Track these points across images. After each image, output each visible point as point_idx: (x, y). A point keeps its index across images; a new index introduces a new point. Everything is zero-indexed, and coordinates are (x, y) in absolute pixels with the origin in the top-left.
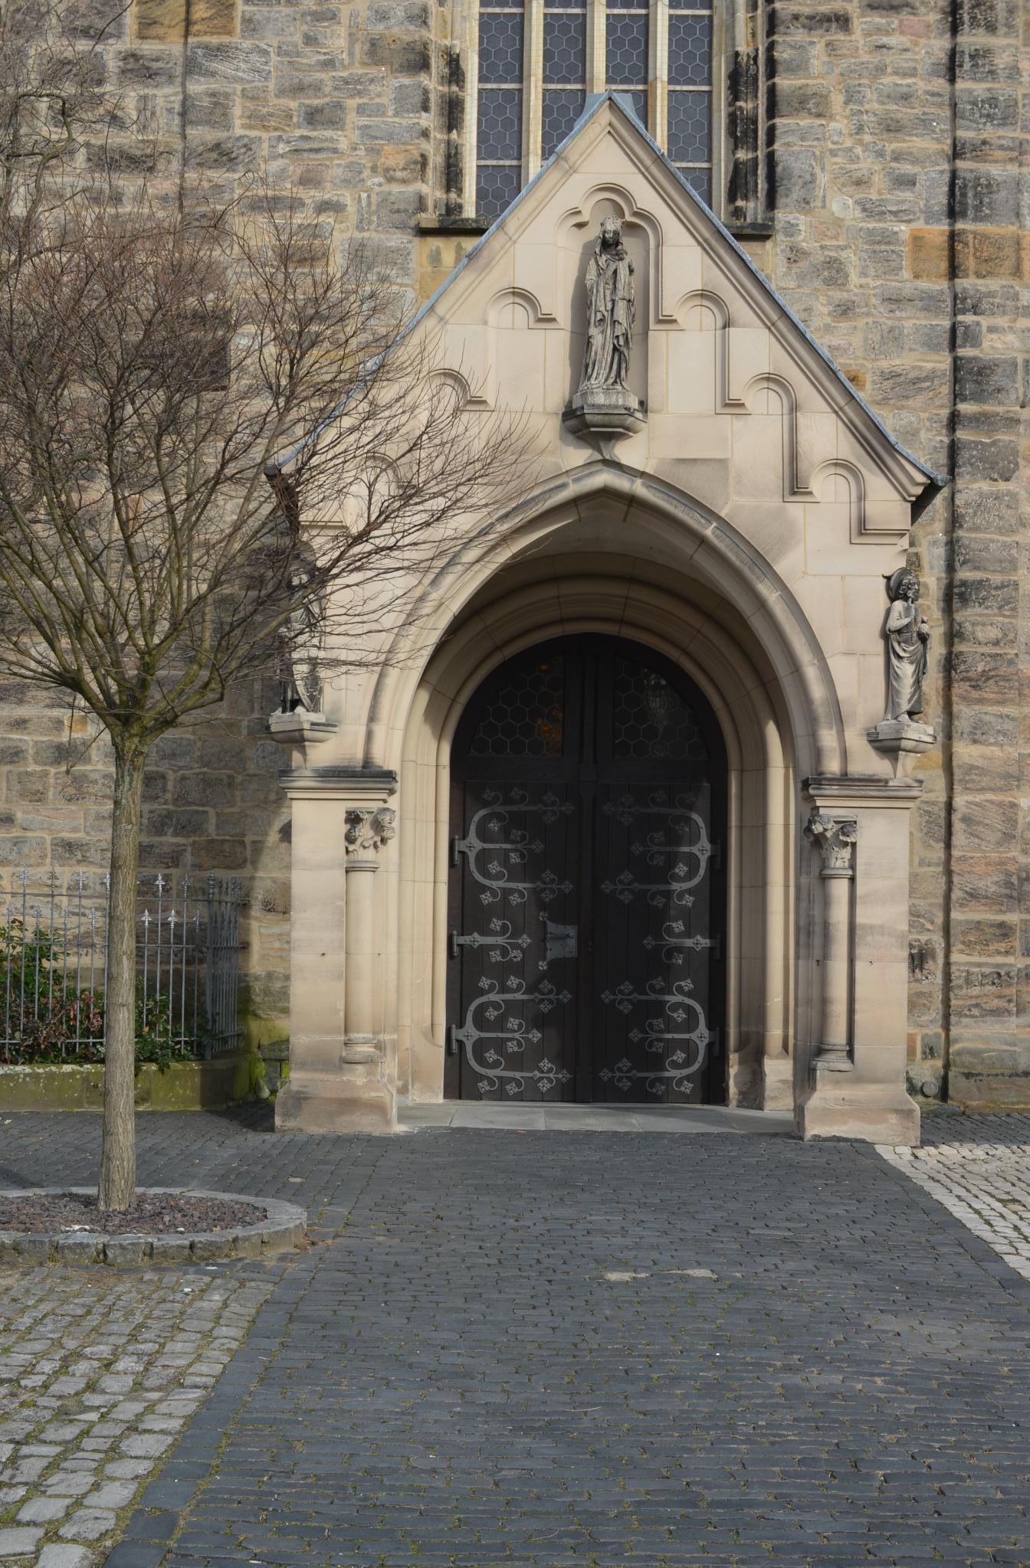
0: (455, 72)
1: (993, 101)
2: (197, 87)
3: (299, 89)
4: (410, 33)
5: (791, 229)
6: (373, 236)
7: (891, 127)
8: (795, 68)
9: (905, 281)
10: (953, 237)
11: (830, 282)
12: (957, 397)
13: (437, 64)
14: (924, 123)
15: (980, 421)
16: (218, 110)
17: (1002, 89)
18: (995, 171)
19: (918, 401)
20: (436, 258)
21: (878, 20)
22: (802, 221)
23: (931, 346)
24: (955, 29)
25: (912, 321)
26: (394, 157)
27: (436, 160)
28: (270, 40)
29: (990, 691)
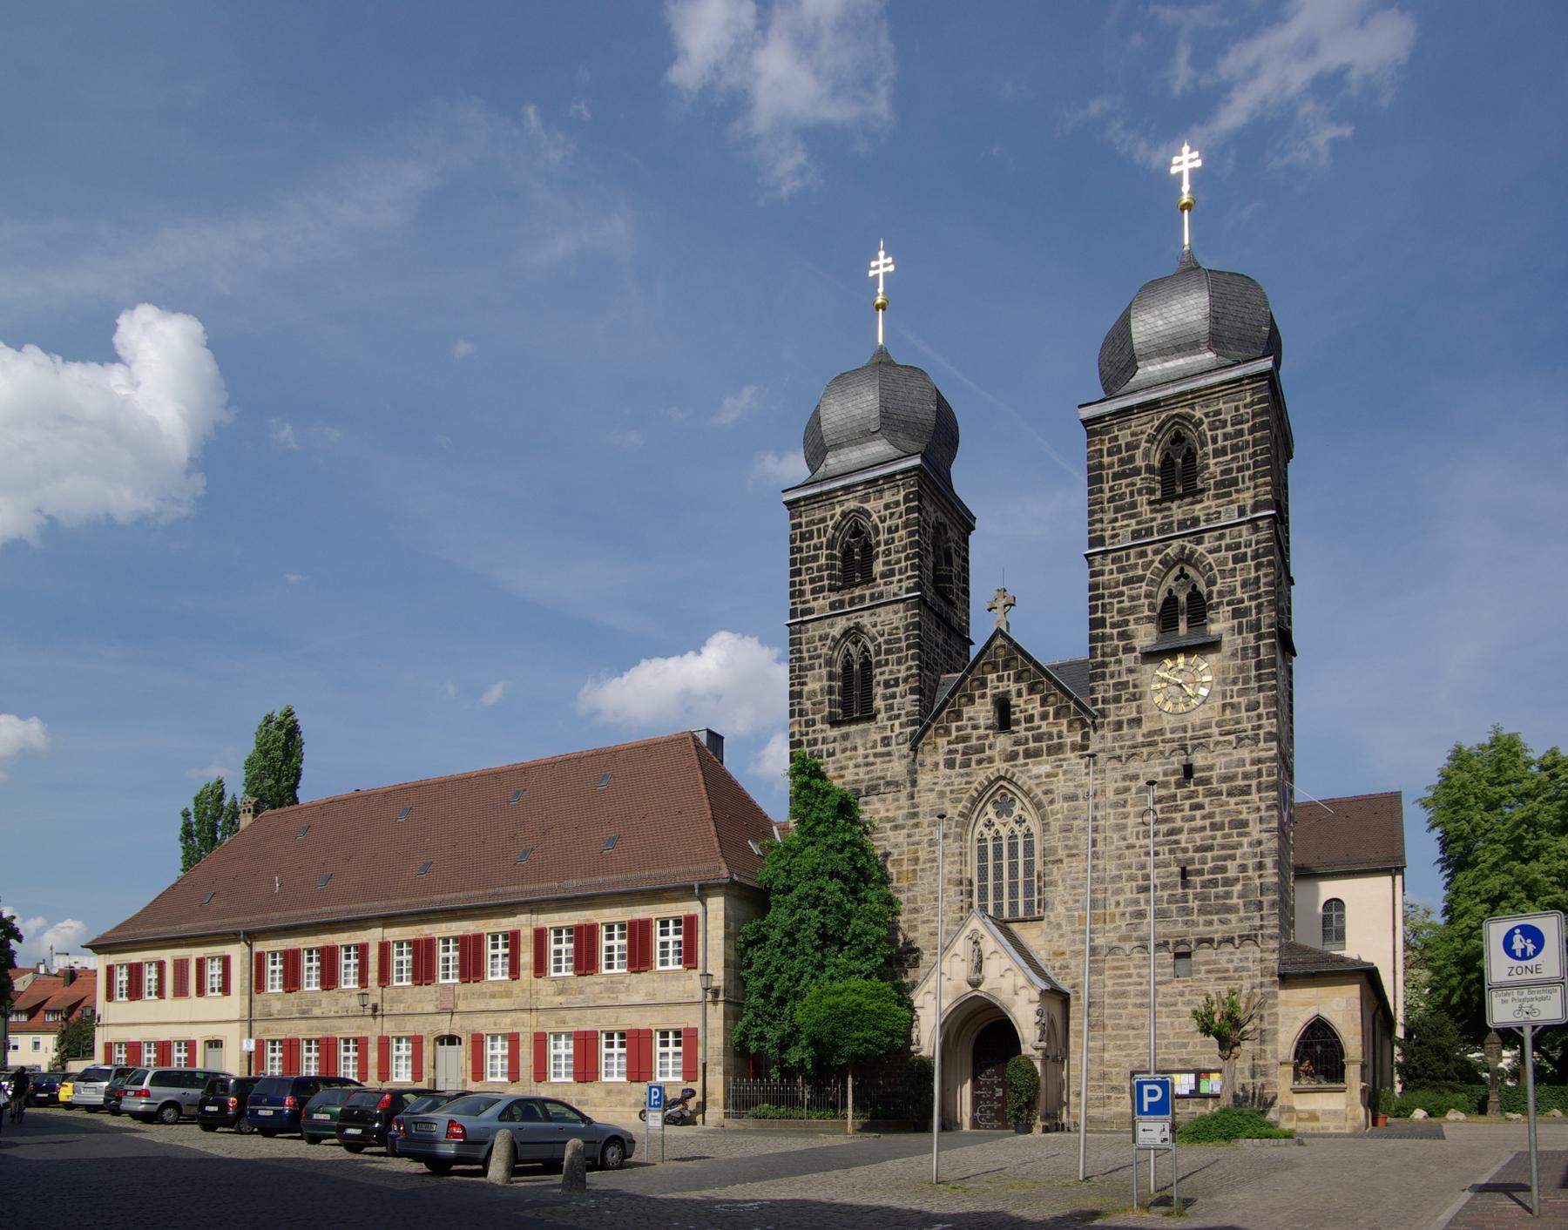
7: (1074, 887)
17: (1101, 874)
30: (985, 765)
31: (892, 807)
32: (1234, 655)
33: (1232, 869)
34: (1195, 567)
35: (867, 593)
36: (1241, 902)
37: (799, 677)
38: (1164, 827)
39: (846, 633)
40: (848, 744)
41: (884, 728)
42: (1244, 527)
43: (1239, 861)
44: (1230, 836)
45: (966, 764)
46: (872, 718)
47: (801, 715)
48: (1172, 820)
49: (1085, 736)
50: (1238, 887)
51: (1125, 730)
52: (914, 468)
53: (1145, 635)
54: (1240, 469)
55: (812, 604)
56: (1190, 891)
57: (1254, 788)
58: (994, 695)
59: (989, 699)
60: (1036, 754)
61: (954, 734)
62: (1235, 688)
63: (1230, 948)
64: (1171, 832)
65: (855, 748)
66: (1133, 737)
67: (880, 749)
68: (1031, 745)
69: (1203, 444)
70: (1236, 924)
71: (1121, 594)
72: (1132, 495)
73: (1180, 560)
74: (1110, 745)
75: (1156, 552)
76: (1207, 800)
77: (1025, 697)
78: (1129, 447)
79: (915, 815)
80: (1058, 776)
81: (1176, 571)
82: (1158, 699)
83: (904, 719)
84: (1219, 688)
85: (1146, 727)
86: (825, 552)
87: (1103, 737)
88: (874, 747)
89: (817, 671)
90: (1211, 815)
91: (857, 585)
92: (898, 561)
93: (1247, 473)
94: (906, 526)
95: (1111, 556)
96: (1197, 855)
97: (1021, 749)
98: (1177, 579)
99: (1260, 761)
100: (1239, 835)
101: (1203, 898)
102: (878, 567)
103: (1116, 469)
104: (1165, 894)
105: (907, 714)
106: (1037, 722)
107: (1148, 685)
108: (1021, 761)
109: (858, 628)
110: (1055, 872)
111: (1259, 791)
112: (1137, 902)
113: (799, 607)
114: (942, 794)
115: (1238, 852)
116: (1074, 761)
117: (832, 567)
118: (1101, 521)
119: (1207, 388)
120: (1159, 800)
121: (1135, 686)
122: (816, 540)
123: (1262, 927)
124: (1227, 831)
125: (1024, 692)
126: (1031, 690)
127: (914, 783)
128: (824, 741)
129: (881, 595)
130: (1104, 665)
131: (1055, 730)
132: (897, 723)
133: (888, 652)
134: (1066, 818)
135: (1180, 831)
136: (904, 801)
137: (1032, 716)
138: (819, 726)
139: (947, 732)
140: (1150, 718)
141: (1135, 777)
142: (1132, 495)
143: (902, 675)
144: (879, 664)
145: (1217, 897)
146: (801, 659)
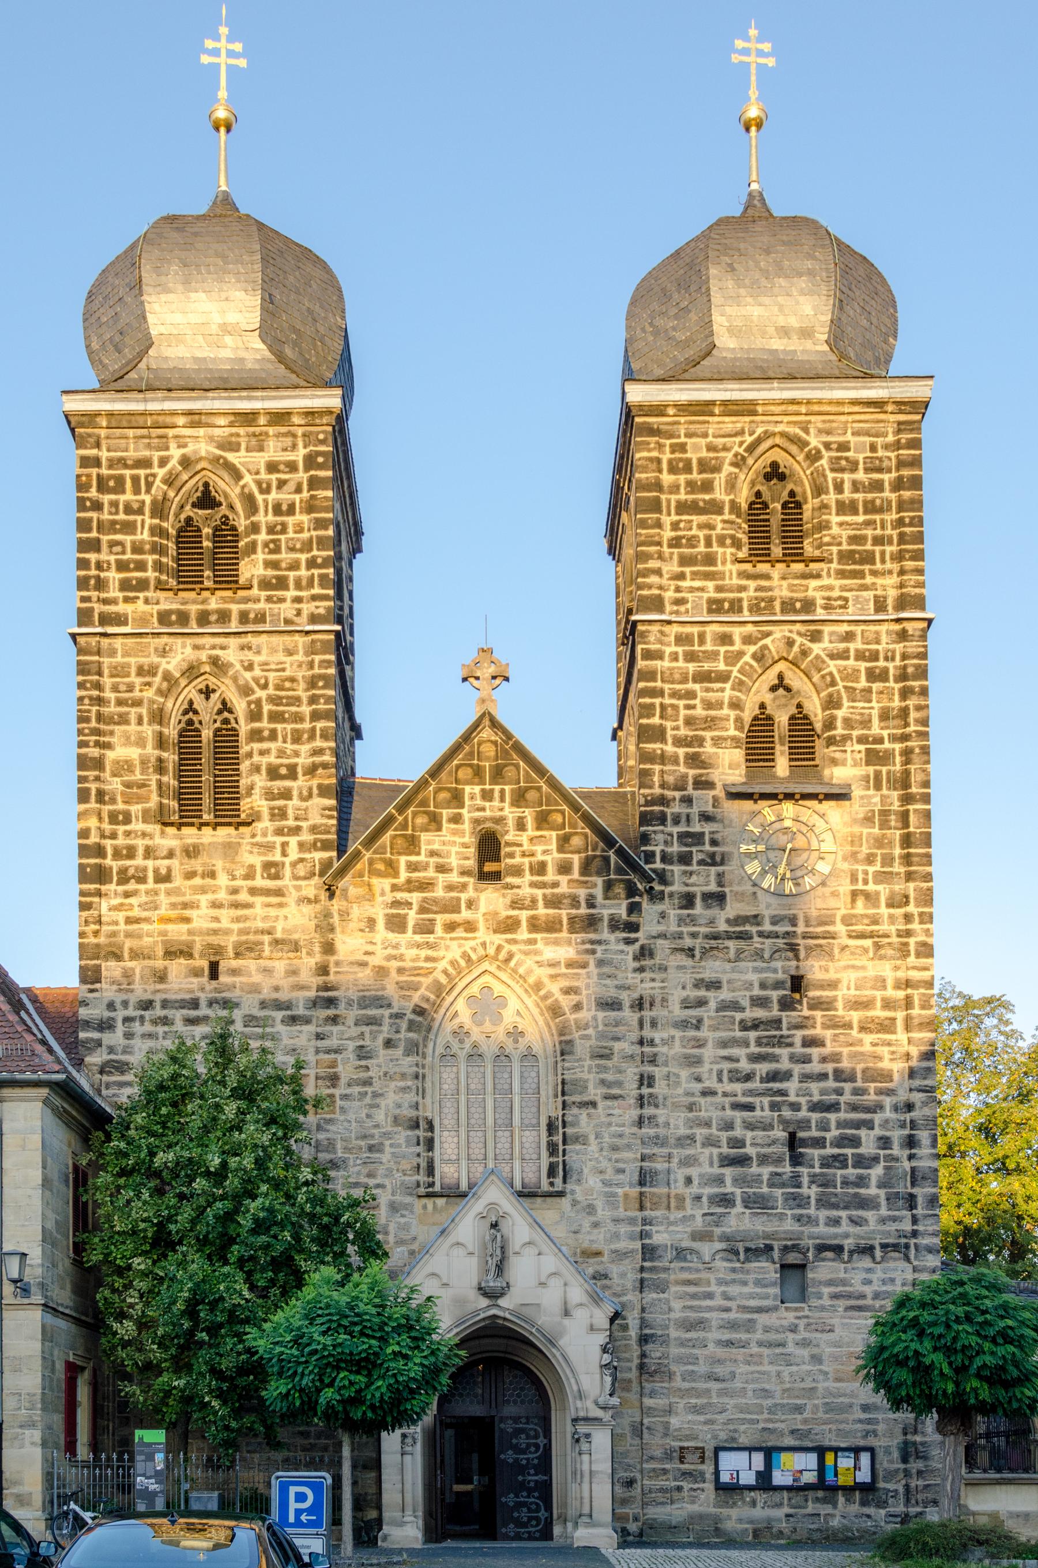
1: (657, 1137)
2: (321, 1136)
3: (365, 1137)
4: (413, 1113)
5: (573, 1192)
6: (398, 1198)
7: (615, 1148)
8: (573, 1125)
9: (621, 1213)
12: (644, 1260)
13: (423, 1124)
15: (652, 1269)
17: (662, 1131)
20: (425, 1207)
21: (609, 1103)
22: (577, 1188)
23: (632, 1238)
24: (642, 1106)
25: (624, 1229)
26: (406, 1165)
27: (423, 1165)
28: (351, 1116)
30: (460, 933)
33: (868, 1147)
35: (235, 608)
36: (882, 1193)
37: (97, 732)
38: (763, 1068)
39: (192, 671)
40: (197, 865)
41: (269, 847)
43: (878, 1131)
45: (425, 928)
48: (775, 1058)
50: (877, 1172)
51: (699, 909)
52: (329, 412)
55: (121, 608)
56: (804, 1170)
57: (900, 1024)
58: (476, 821)
59: (467, 826)
61: (404, 875)
63: (866, 1262)
64: (774, 1076)
65: (212, 875)
66: (712, 922)
67: (260, 882)
68: (542, 911)
70: (875, 1225)
74: (673, 928)
76: (828, 1034)
79: (331, 1002)
82: (753, 868)
83: (306, 837)
85: (733, 908)
86: (148, 521)
87: (663, 915)
88: (250, 876)
89: (133, 728)
92: (294, 566)
94: (310, 507)
95: (675, 629)
96: (815, 1116)
97: (524, 915)
101: (826, 1183)
102: (252, 568)
104: (766, 1171)
105: (313, 829)
106: (551, 876)
107: (736, 844)
108: (523, 934)
110: (584, 1122)
111: (908, 1028)
112: (720, 1180)
113: (98, 608)
115: (877, 1118)
116: (614, 947)
117: (161, 550)
120: (756, 1025)
121: (714, 843)
122: (128, 496)
123: (915, 1234)
125: (530, 823)
126: (543, 820)
127: (329, 948)
128: (149, 853)
129: (261, 618)
131: (582, 893)
132: (293, 841)
133: (275, 717)
134: (602, 1036)
135: (787, 1076)
138: (137, 826)
140: (740, 896)
141: (715, 985)
143: (303, 761)
144: (256, 735)
145: (845, 1183)
146: (100, 701)
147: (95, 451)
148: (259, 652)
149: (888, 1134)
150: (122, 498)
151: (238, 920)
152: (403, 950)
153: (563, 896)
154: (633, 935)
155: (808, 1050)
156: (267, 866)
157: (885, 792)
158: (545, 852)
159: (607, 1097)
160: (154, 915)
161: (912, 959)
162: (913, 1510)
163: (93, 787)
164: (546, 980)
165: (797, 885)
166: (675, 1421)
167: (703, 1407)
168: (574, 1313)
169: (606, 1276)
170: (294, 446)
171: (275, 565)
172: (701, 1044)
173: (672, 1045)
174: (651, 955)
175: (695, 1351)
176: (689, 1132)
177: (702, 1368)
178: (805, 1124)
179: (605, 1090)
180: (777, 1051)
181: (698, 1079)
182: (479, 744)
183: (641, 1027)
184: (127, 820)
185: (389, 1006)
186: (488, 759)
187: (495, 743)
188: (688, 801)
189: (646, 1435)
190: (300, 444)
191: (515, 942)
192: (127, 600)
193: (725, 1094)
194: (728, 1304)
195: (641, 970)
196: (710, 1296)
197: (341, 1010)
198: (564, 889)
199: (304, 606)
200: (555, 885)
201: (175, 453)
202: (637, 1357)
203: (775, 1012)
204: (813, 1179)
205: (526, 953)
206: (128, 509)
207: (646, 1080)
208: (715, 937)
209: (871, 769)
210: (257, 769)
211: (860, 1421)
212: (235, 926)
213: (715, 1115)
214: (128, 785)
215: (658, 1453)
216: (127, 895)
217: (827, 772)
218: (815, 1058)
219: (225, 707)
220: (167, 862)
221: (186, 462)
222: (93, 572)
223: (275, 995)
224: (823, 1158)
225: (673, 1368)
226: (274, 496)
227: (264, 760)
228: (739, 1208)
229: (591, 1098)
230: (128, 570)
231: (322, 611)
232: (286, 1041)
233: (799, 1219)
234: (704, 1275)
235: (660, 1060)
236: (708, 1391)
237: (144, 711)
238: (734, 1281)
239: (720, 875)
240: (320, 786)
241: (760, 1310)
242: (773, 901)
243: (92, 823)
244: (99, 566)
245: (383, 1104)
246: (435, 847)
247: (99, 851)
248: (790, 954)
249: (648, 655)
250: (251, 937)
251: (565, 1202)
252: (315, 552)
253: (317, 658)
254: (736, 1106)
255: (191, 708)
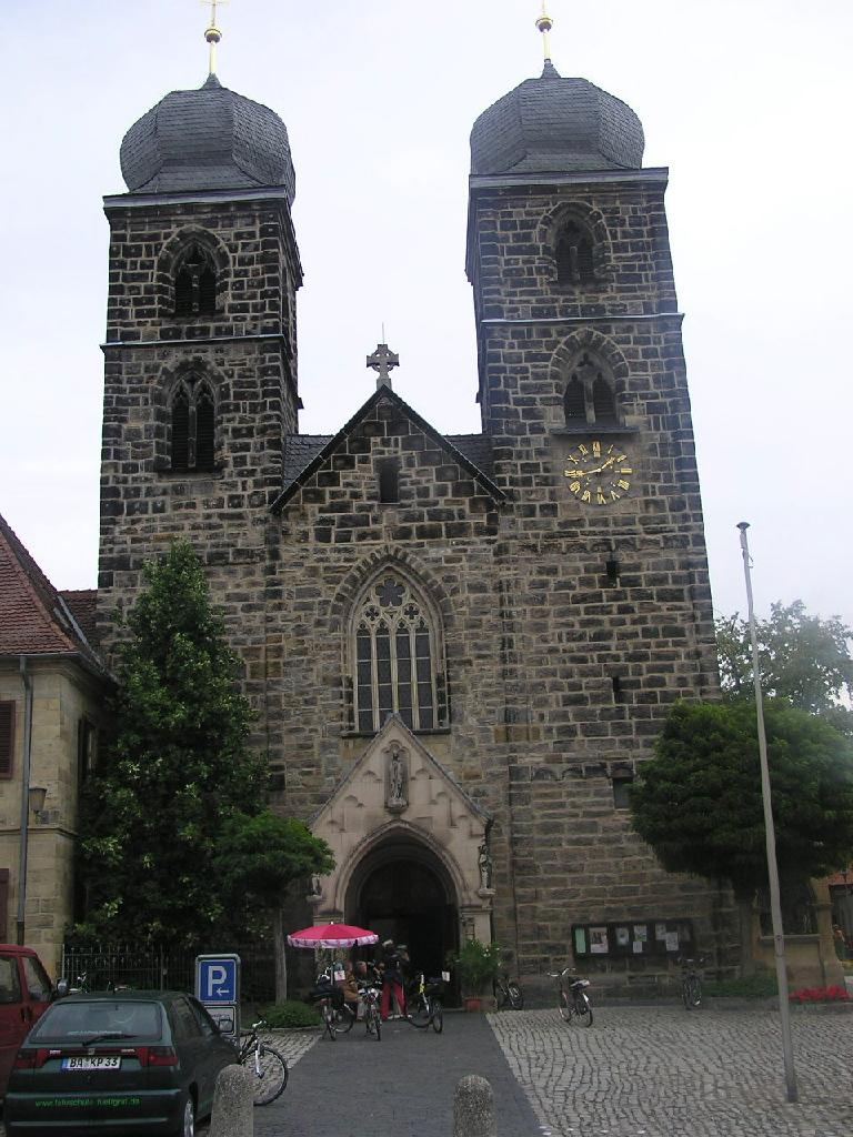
0: (351, 684)
3: (302, 694)
4: (336, 675)
7: (486, 695)
10: (507, 729)
11: (470, 746)
14: (497, 693)
15: (519, 787)
16: (277, 701)
18: (519, 707)
19: (499, 781)
24: (505, 662)
25: (496, 756)
26: (332, 713)
29: (525, 871)
31: (244, 581)
32: (653, 450)
34: (603, 355)
35: (212, 325)
37: (115, 411)
38: (590, 631)
41: (234, 485)
42: (651, 324)
43: (677, 674)
44: (666, 644)
46: (218, 469)
47: (118, 455)
49: (492, 518)
51: (538, 517)
53: (555, 419)
54: (642, 268)
58: (377, 462)
60: (432, 534)
61: (328, 500)
62: (657, 485)
64: (598, 637)
66: (549, 523)
67: (226, 510)
69: (602, 237)
71: (525, 370)
72: (530, 272)
73: (585, 345)
75: (561, 334)
76: (636, 604)
77: (417, 468)
78: (524, 225)
79: (278, 594)
80: (461, 562)
81: (579, 357)
82: (575, 487)
83: (259, 476)
84: (640, 483)
85: (562, 516)
87: (513, 522)
89: (141, 407)
90: (642, 620)
91: (197, 315)
93: (650, 273)
96: (630, 664)
97: (415, 525)
98: (581, 365)
99: (687, 565)
100: (676, 644)
101: (641, 713)
102: (226, 299)
103: (511, 243)
105: (264, 471)
106: (432, 497)
109: (200, 365)
110: (463, 676)
112: (564, 716)
114: (313, 571)
115: (676, 663)
118: (498, 292)
119: (603, 184)
120: (584, 598)
122: (143, 258)
124: (661, 639)
126: (425, 460)
127: (275, 555)
128: (149, 492)
129: (229, 331)
130: (511, 442)
132: (250, 481)
133: (238, 396)
135: (609, 636)
136: (258, 577)
137: (427, 489)
138: (141, 474)
139: (319, 497)
141: (553, 571)
142: (530, 273)
143: (257, 424)
144: (225, 409)
147: (123, 232)
148: (227, 354)
149: (685, 675)
150: (139, 259)
151: (211, 537)
152: (328, 554)
153: (441, 511)
154: (493, 538)
155: (622, 616)
156: (232, 498)
157: (662, 431)
158: (428, 481)
159: (479, 657)
160: (151, 536)
161: (690, 548)
162: (724, 968)
163: (112, 448)
164: (432, 572)
165: (606, 497)
166: (540, 906)
167: (562, 893)
168: (457, 823)
169: (484, 794)
170: (253, 223)
171: (240, 297)
172: (545, 614)
173: (522, 614)
174: (507, 551)
175: (554, 849)
176: (539, 680)
177: (559, 862)
178: (624, 671)
179: (477, 652)
180: (601, 617)
181: (545, 641)
182: (380, 408)
183: (502, 604)
184: (135, 468)
185: (319, 595)
186: (386, 418)
187: (389, 407)
188: (527, 442)
189: (519, 918)
190: (258, 222)
191: (408, 545)
192: (139, 324)
193: (565, 651)
194: (576, 811)
195: (500, 562)
196: (562, 805)
197: (284, 598)
198: (441, 506)
199: (258, 322)
200: (436, 503)
201: (175, 230)
202: (511, 865)
203: (598, 589)
204: (633, 712)
205: (417, 554)
206: (143, 266)
207: (507, 643)
208: (552, 537)
209: (651, 416)
210: (226, 431)
211: (679, 898)
212: (209, 542)
213: (558, 666)
214: (136, 446)
215: (528, 931)
216: (134, 522)
217: (621, 419)
218: (628, 621)
219: (205, 389)
220: (161, 498)
221: (181, 235)
222: (118, 307)
223: (237, 591)
224: (638, 696)
225: (537, 863)
226: (240, 253)
227: (230, 426)
228: (580, 737)
229: (468, 657)
230: (143, 304)
231: (271, 325)
232: (244, 623)
233: (623, 742)
234: (557, 790)
235: (517, 627)
236: (564, 880)
237: (149, 396)
238: (578, 793)
239: (552, 493)
240: (268, 442)
241: (599, 814)
242: (591, 510)
243: (111, 473)
244: (123, 303)
245: (315, 668)
246: (350, 480)
247: (115, 492)
248: (605, 548)
249: (493, 344)
250: (221, 550)
251: (452, 738)
252: (266, 288)
253: (267, 355)
254: (573, 660)
255: (181, 392)
